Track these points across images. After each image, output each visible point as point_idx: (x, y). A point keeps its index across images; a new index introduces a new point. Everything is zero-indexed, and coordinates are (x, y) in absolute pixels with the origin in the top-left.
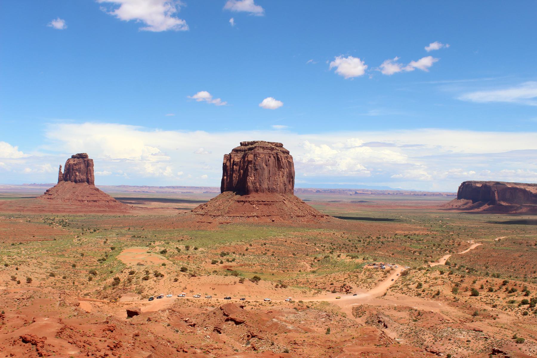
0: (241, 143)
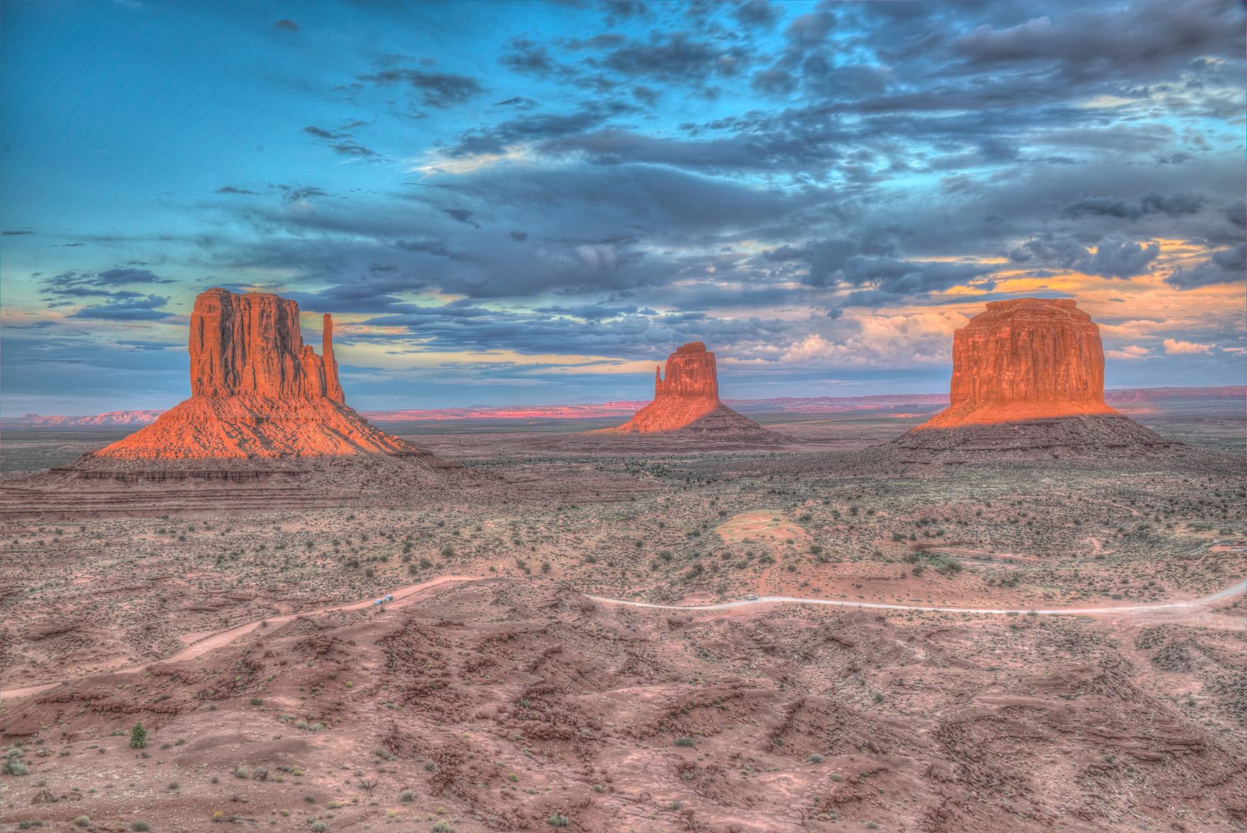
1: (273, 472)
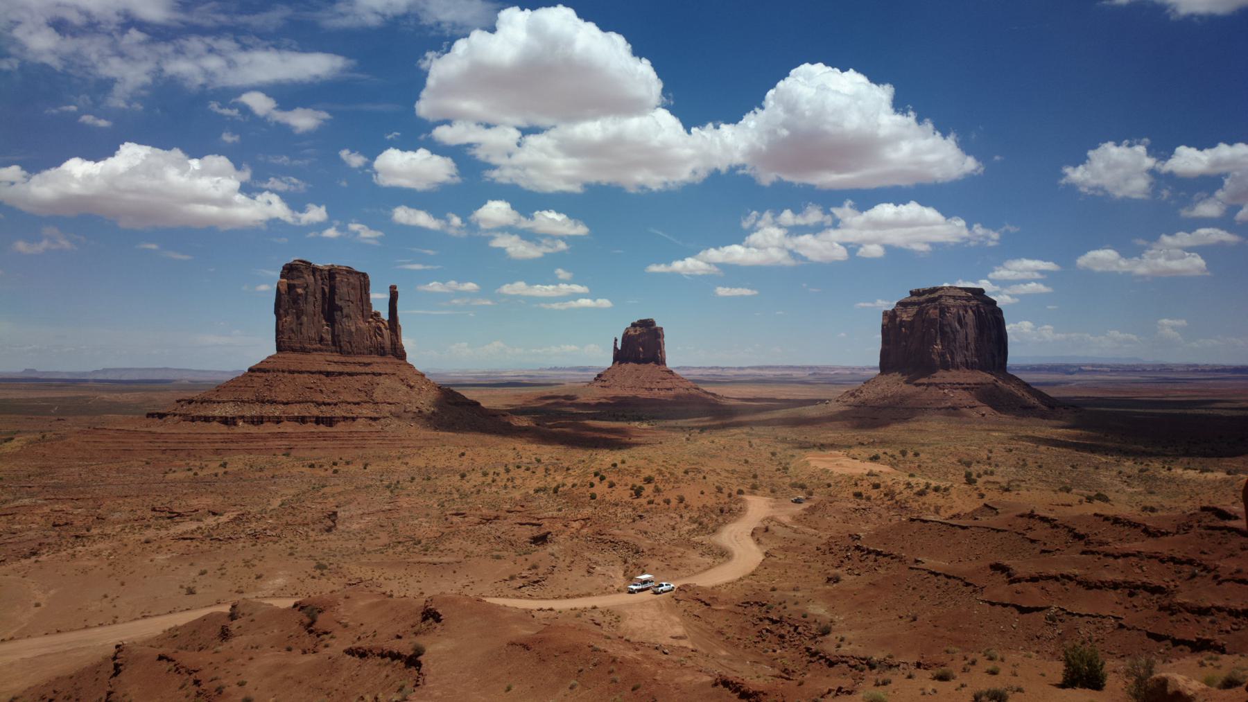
0: (911, 292)
1: (357, 418)
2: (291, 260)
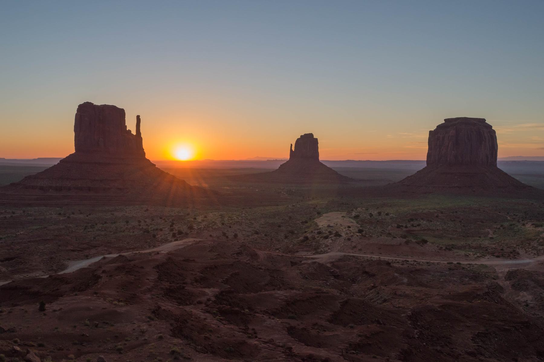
0: (445, 120)
2: (82, 103)
